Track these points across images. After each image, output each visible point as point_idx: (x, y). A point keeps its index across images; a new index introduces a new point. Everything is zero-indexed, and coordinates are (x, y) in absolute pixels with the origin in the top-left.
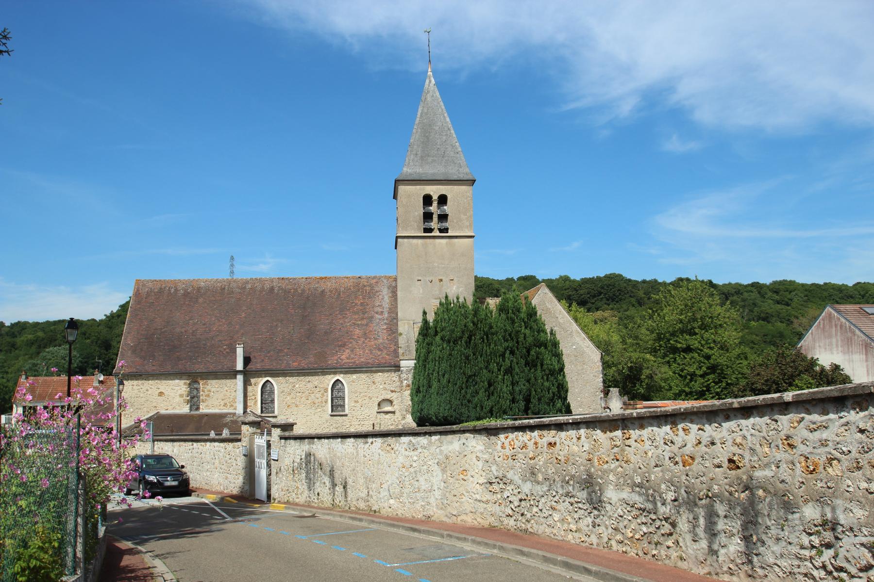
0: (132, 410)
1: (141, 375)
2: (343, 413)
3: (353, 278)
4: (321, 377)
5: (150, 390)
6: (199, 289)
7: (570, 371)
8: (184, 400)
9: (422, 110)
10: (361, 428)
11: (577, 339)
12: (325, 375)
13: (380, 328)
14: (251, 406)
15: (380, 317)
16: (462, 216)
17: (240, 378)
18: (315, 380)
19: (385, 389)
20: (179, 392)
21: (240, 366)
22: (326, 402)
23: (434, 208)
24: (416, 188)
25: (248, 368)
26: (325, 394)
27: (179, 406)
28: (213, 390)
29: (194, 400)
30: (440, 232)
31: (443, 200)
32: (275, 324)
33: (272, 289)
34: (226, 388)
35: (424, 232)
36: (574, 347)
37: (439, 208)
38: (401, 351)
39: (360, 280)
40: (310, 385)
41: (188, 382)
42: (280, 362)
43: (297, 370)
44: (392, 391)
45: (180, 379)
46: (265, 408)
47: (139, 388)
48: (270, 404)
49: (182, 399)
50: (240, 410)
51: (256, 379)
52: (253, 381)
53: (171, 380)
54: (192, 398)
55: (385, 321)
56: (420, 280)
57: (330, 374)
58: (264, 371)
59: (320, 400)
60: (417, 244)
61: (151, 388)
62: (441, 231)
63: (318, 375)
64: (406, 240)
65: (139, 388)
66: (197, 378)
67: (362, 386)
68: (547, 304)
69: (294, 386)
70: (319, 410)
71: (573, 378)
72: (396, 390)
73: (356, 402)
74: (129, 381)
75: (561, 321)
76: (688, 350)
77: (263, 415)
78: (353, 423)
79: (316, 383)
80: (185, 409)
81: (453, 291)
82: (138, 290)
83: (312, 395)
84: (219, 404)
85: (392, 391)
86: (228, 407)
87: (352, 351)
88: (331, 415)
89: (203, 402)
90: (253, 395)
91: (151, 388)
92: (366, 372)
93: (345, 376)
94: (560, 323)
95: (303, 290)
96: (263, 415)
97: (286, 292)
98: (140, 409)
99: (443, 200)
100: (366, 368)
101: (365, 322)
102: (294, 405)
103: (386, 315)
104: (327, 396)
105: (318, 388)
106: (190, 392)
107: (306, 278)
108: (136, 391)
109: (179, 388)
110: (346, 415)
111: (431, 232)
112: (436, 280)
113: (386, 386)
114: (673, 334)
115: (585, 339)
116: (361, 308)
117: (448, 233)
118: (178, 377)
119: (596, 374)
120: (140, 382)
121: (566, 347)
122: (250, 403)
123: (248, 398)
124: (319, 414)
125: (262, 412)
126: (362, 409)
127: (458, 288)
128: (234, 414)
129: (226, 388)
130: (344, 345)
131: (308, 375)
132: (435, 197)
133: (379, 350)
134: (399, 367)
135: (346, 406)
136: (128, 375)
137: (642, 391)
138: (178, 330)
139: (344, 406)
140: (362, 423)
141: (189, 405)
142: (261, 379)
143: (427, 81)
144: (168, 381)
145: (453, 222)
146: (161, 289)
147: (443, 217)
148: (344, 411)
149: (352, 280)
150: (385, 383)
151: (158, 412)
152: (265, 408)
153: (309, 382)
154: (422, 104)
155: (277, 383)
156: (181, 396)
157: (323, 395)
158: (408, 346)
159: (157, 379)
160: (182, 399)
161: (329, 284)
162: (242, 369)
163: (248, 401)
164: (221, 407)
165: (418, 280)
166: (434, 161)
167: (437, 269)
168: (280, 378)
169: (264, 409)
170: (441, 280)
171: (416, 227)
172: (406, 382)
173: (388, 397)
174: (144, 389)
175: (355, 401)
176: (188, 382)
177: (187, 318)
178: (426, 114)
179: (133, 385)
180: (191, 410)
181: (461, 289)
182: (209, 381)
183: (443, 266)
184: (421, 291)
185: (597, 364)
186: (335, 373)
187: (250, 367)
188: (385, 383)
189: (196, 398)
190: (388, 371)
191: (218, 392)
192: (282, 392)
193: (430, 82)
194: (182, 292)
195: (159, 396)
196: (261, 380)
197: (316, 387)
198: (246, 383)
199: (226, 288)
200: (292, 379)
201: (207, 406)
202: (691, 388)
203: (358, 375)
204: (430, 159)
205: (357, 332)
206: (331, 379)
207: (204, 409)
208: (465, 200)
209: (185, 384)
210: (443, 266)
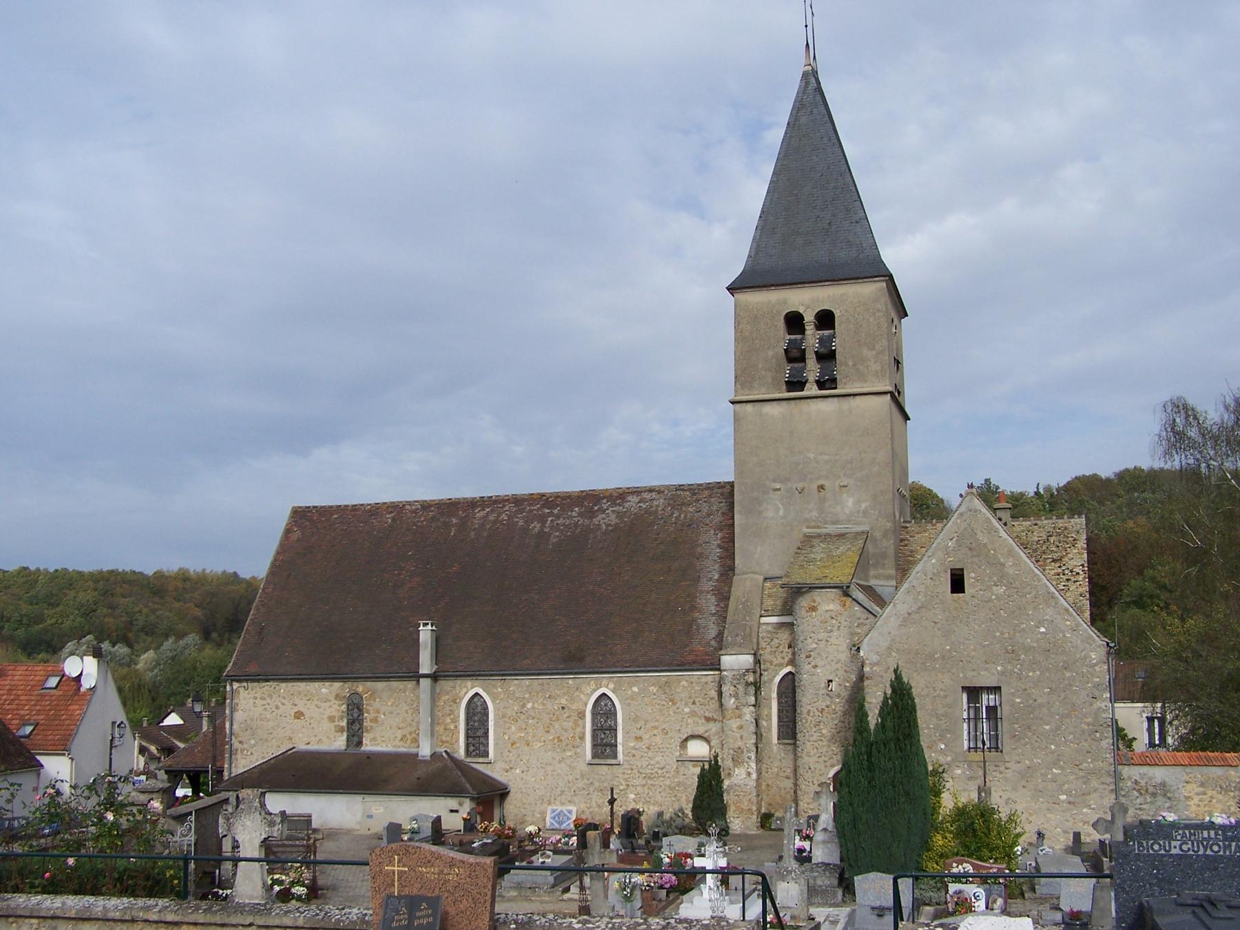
2: (613, 762)
8: (335, 726)
16: (866, 352)
19: (693, 714)
20: (328, 713)
22: (582, 738)
26: (580, 722)
28: (383, 709)
30: (820, 389)
31: (826, 319)
35: (789, 391)
36: (1043, 630)
40: (553, 706)
44: (708, 719)
47: (264, 702)
48: (482, 739)
56: (779, 490)
61: (283, 704)
62: (821, 385)
69: (524, 706)
70: (569, 754)
72: (715, 717)
73: (639, 738)
75: (1011, 571)
80: (339, 743)
81: (847, 511)
85: (708, 719)
86: (409, 742)
91: (283, 704)
96: (469, 760)
99: (826, 319)
104: (584, 727)
108: (260, 709)
109: (328, 704)
111: (803, 390)
113: (696, 708)
117: (836, 388)
124: (568, 762)
125: (468, 753)
126: (650, 754)
127: (858, 502)
132: (809, 317)
135: (620, 748)
145: (846, 365)
147: (827, 356)
150: (694, 703)
155: (494, 698)
156: (331, 719)
157: (576, 724)
160: (332, 725)
170: (821, 487)
171: (769, 380)
173: (700, 730)
179: (255, 698)
181: (864, 505)
183: (826, 457)
184: (781, 512)
188: (694, 703)
191: (391, 713)
197: (563, 708)
201: (374, 739)
207: (370, 745)
210: (826, 457)
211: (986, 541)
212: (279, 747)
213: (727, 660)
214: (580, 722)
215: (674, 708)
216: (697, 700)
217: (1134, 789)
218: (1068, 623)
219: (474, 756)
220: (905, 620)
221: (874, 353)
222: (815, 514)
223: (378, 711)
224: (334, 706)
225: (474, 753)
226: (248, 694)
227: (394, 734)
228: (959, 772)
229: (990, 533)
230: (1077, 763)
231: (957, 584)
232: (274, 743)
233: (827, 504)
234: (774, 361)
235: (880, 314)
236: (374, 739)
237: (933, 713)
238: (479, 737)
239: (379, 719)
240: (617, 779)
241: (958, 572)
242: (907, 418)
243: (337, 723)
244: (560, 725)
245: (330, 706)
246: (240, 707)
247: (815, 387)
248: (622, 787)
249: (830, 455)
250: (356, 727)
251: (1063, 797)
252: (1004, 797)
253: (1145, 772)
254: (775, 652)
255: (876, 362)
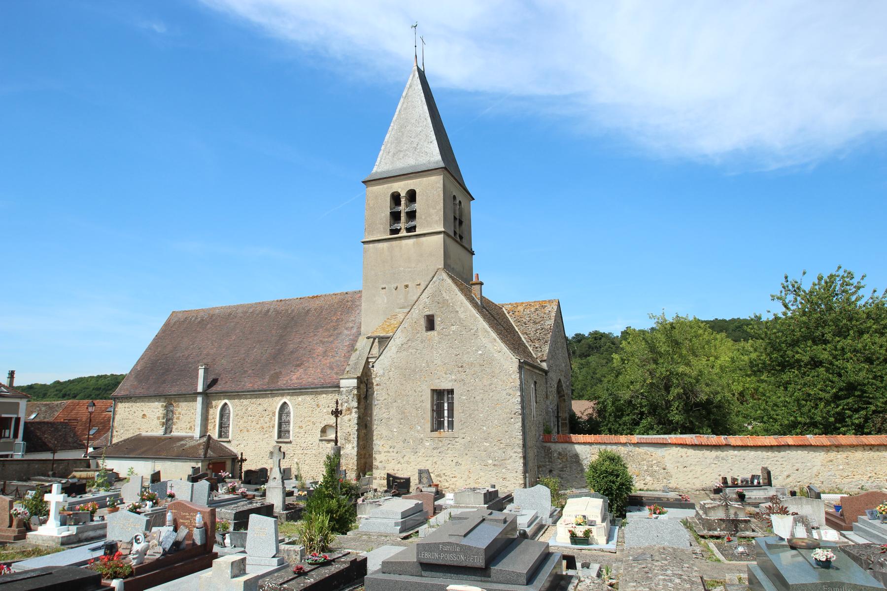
0: (122, 431)
1: (131, 398)
3: (341, 294)
4: (270, 399)
5: (137, 412)
6: (213, 316)
7: (473, 388)
8: (160, 422)
9: (402, 106)
10: (303, 457)
11: (484, 341)
12: (274, 397)
13: (342, 345)
14: (210, 430)
15: (349, 333)
16: (432, 211)
17: (200, 399)
18: (266, 402)
20: (157, 415)
21: (200, 389)
22: (273, 427)
23: (403, 208)
24: (384, 187)
25: (208, 391)
28: (183, 412)
29: (168, 422)
30: (407, 232)
31: (412, 196)
32: (255, 345)
33: (268, 311)
37: (407, 206)
38: (347, 369)
39: (346, 295)
40: (260, 408)
41: (164, 404)
42: (239, 383)
43: (248, 392)
45: (159, 401)
46: (224, 432)
47: (129, 410)
50: (197, 434)
51: (216, 401)
52: (214, 403)
53: (153, 402)
54: (168, 420)
55: (351, 337)
56: (385, 288)
57: (278, 396)
58: (221, 393)
59: (268, 424)
60: (383, 249)
61: (138, 410)
62: (409, 230)
63: (268, 397)
64: (371, 245)
65: (129, 410)
66: (171, 400)
67: (306, 410)
68: (444, 295)
69: (247, 410)
70: (267, 436)
71: (477, 398)
73: (301, 427)
75: (462, 316)
76: (815, 363)
77: (219, 440)
78: (297, 452)
79: (265, 406)
80: (159, 432)
82: (169, 321)
83: (262, 419)
84: (185, 427)
87: (306, 370)
88: (277, 442)
90: (213, 418)
91: (138, 410)
92: (312, 393)
93: (292, 398)
94: (460, 319)
95: (293, 311)
97: (277, 312)
100: (312, 388)
101: (331, 339)
102: (245, 429)
103: (354, 330)
104: (274, 421)
105: (266, 411)
106: (167, 414)
107: (300, 299)
108: (127, 413)
109: (157, 410)
110: (290, 442)
111: (398, 234)
112: (401, 287)
114: (795, 343)
115: (495, 340)
116: (334, 324)
117: (415, 231)
118: (158, 399)
119: (511, 392)
120: (130, 404)
121: (468, 353)
122: (210, 427)
123: (209, 422)
125: (220, 436)
126: (306, 436)
128: (192, 438)
129: (193, 411)
130: (299, 366)
131: (259, 398)
132: (403, 194)
133: (331, 368)
134: (339, 387)
135: (291, 433)
136: (122, 398)
137: (677, 418)
138: (178, 355)
139: (289, 432)
140: (305, 452)
141: (164, 428)
142: (220, 401)
143: (411, 76)
144: (150, 404)
146: (186, 318)
147: (412, 215)
148: (289, 438)
149: (339, 297)
150: (328, 407)
151: (140, 434)
152: (224, 432)
153: (260, 404)
154: (402, 100)
155: (235, 406)
157: (271, 418)
158: (356, 364)
159: (142, 402)
161: (318, 302)
162: (201, 391)
163: (209, 425)
164: (187, 430)
165: (382, 289)
166: (405, 155)
167: (403, 273)
168: (236, 400)
169: (223, 433)
170: (407, 286)
171: (382, 229)
172: (346, 404)
175: (300, 427)
176: (164, 404)
177: (191, 343)
178: (405, 109)
179: (125, 407)
180: (165, 433)
182: (181, 404)
183: (410, 269)
184: (385, 301)
185: (513, 376)
186: (282, 395)
187: (214, 389)
188: (328, 407)
189: (171, 421)
190: (332, 392)
191: (186, 414)
192: (237, 415)
193: (414, 76)
194: (199, 319)
195: (143, 418)
196: (220, 403)
197: (265, 410)
198: (206, 407)
199: (233, 314)
200: (246, 402)
201: (177, 429)
202: (812, 418)
203: (303, 397)
204: (402, 155)
205: (320, 349)
206: (279, 402)
207: (175, 433)
208: (435, 192)
210: (410, 269)
211: (448, 298)
213: (343, 383)
214: (273, 418)
215: (319, 409)
216: (330, 405)
217: (559, 458)
218: (496, 348)
219: (224, 438)
220: (400, 348)
221: (436, 211)
222: (402, 301)
225: (224, 436)
227: (186, 425)
228: (428, 444)
229: (450, 293)
230: (499, 439)
231: (430, 324)
232: (132, 431)
233: (409, 295)
234: (384, 219)
235: (440, 189)
236: (177, 429)
237: (414, 406)
238: (226, 427)
239: (180, 418)
240: (289, 450)
241: (431, 318)
242: (473, 253)
243: (161, 420)
244: (264, 420)
245: (159, 411)
246: (118, 413)
247: (405, 231)
248: (291, 455)
249: (411, 268)
250: (170, 422)
251: (490, 462)
252: (455, 461)
253: (566, 447)
254: (375, 378)
255: (436, 215)
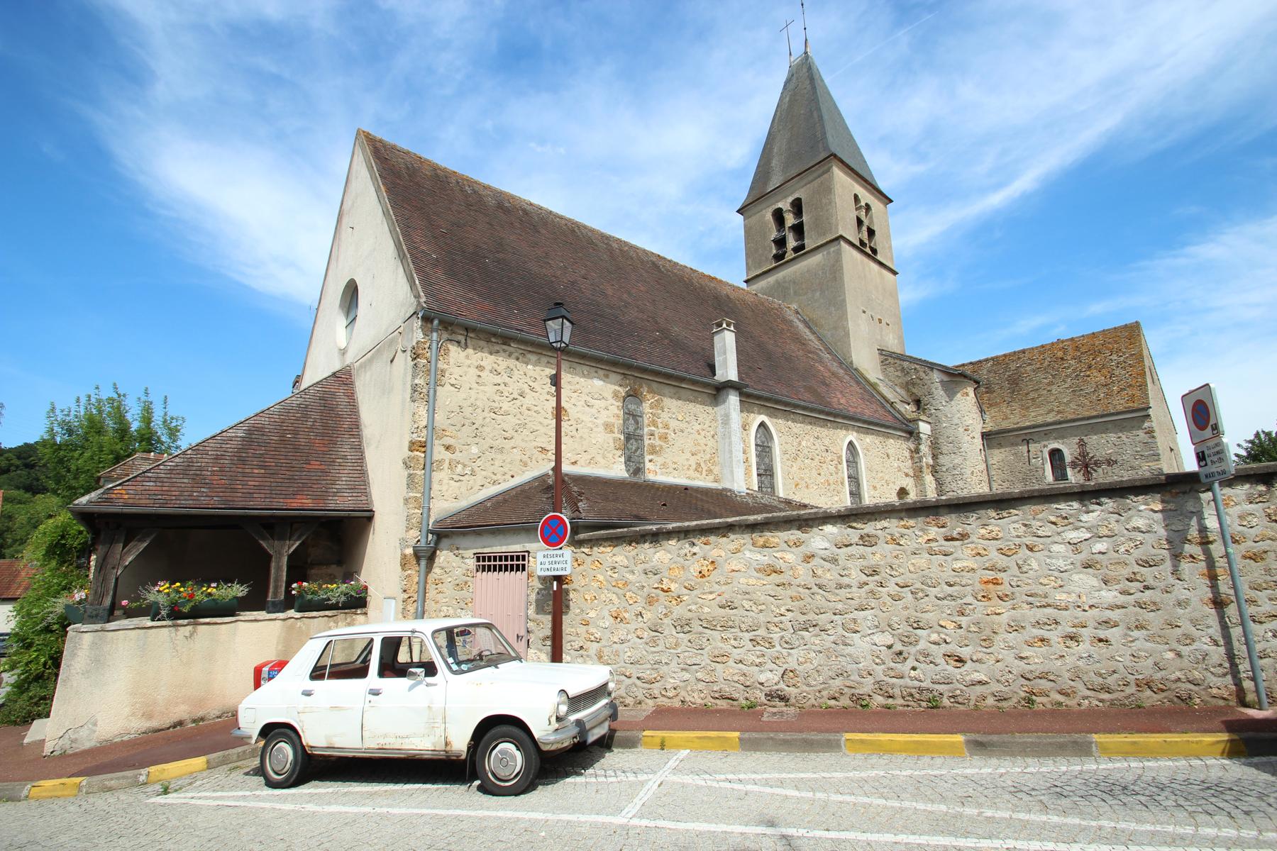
5: (530, 394)
8: (615, 440)
20: (605, 417)
26: (839, 466)
27: (604, 457)
28: (673, 424)
34: (697, 427)
40: (819, 446)
47: (498, 379)
49: (610, 438)
53: (584, 376)
61: (532, 389)
65: (498, 379)
74: (470, 351)
80: (616, 469)
89: (653, 451)
98: (501, 450)
108: (491, 390)
109: (602, 403)
120: (502, 362)
144: (577, 379)
156: (608, 427)
160: (610, 438)
164: (691, 473)
174: (514, 388)
207: (658, 472)
209: (616, 395)
212: (525, 465)
214: (839, 466)
223: (666, 426)
224: (610, 408)
226: (467, 357)
